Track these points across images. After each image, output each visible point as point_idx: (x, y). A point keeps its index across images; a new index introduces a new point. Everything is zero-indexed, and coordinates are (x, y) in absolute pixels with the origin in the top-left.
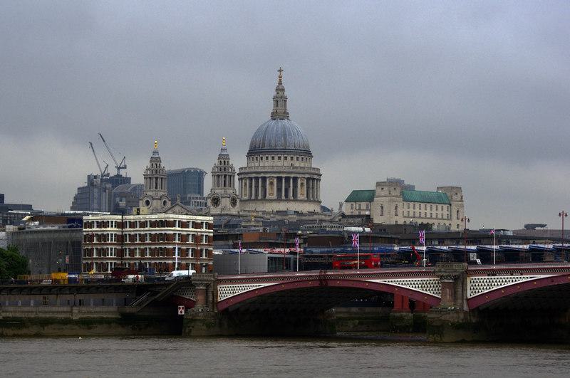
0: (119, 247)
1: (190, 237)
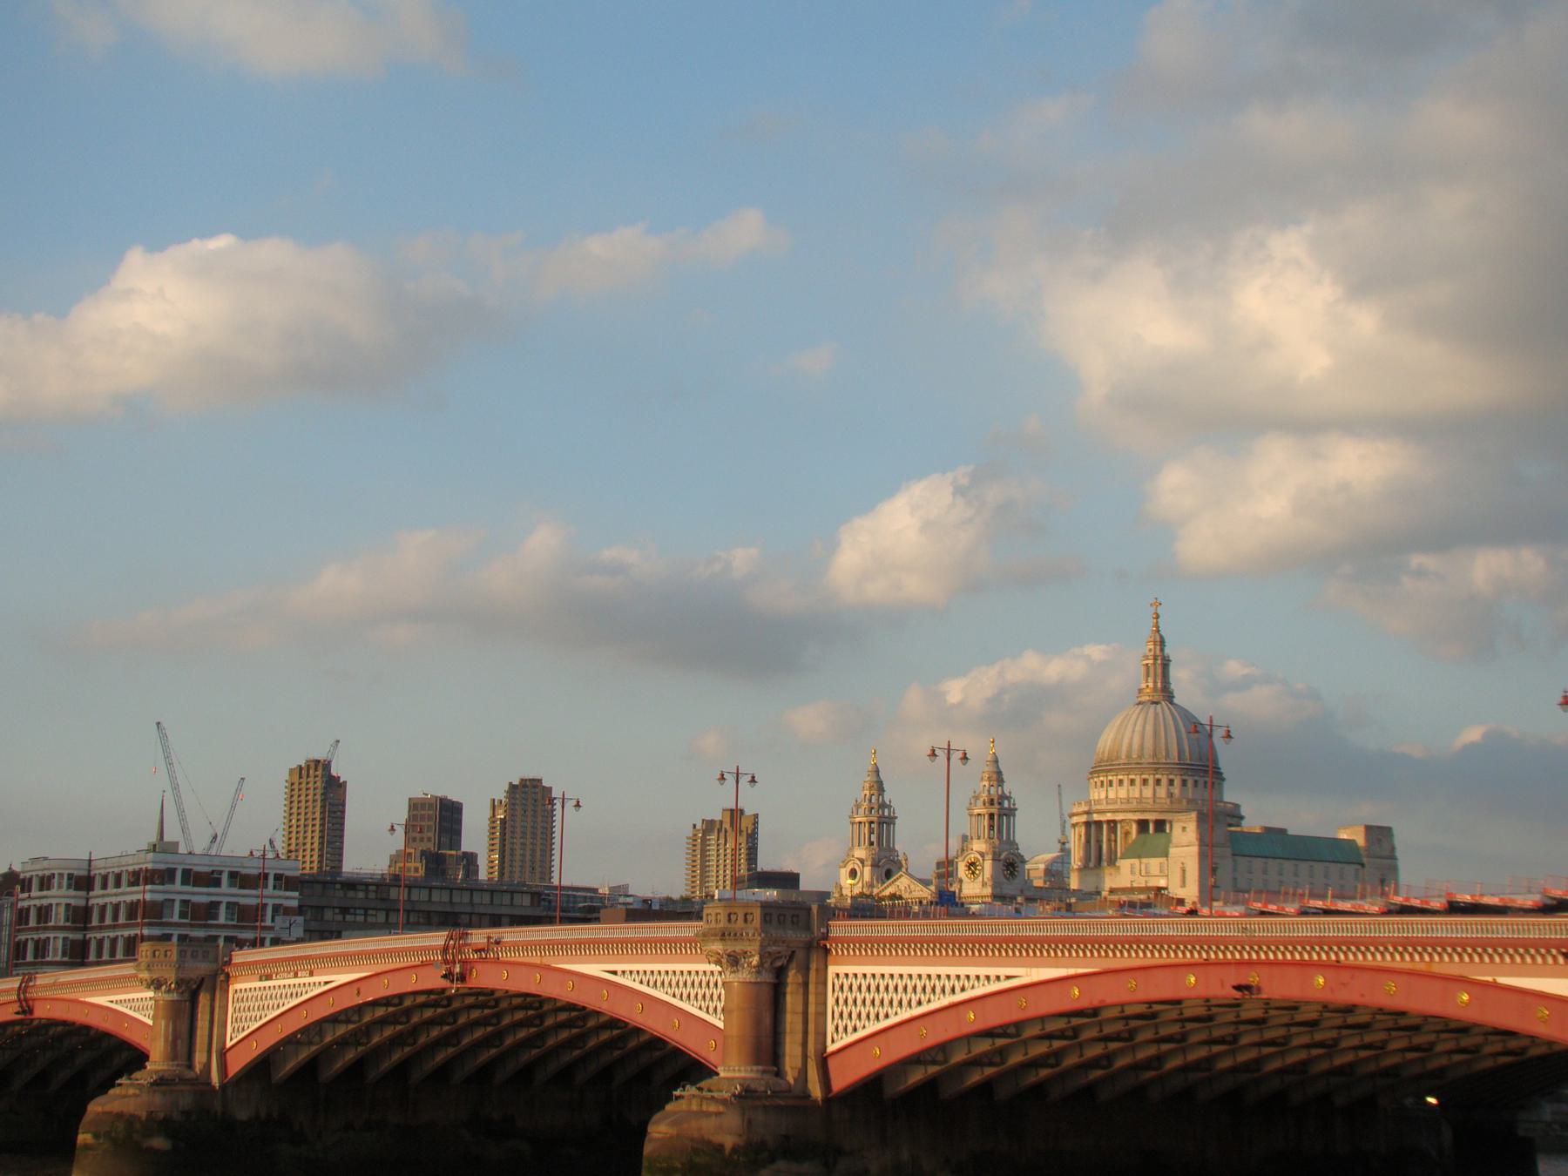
0: (78, 936)
1: (223, 909)
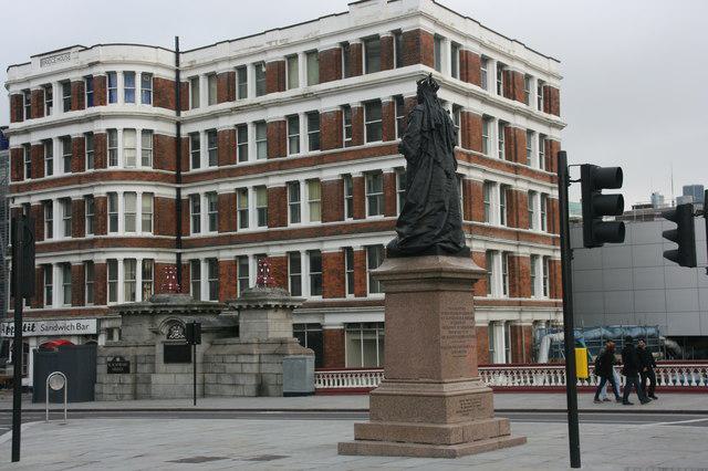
0: (168, 192)
